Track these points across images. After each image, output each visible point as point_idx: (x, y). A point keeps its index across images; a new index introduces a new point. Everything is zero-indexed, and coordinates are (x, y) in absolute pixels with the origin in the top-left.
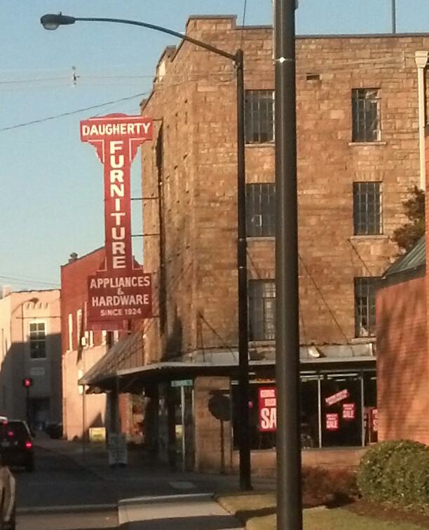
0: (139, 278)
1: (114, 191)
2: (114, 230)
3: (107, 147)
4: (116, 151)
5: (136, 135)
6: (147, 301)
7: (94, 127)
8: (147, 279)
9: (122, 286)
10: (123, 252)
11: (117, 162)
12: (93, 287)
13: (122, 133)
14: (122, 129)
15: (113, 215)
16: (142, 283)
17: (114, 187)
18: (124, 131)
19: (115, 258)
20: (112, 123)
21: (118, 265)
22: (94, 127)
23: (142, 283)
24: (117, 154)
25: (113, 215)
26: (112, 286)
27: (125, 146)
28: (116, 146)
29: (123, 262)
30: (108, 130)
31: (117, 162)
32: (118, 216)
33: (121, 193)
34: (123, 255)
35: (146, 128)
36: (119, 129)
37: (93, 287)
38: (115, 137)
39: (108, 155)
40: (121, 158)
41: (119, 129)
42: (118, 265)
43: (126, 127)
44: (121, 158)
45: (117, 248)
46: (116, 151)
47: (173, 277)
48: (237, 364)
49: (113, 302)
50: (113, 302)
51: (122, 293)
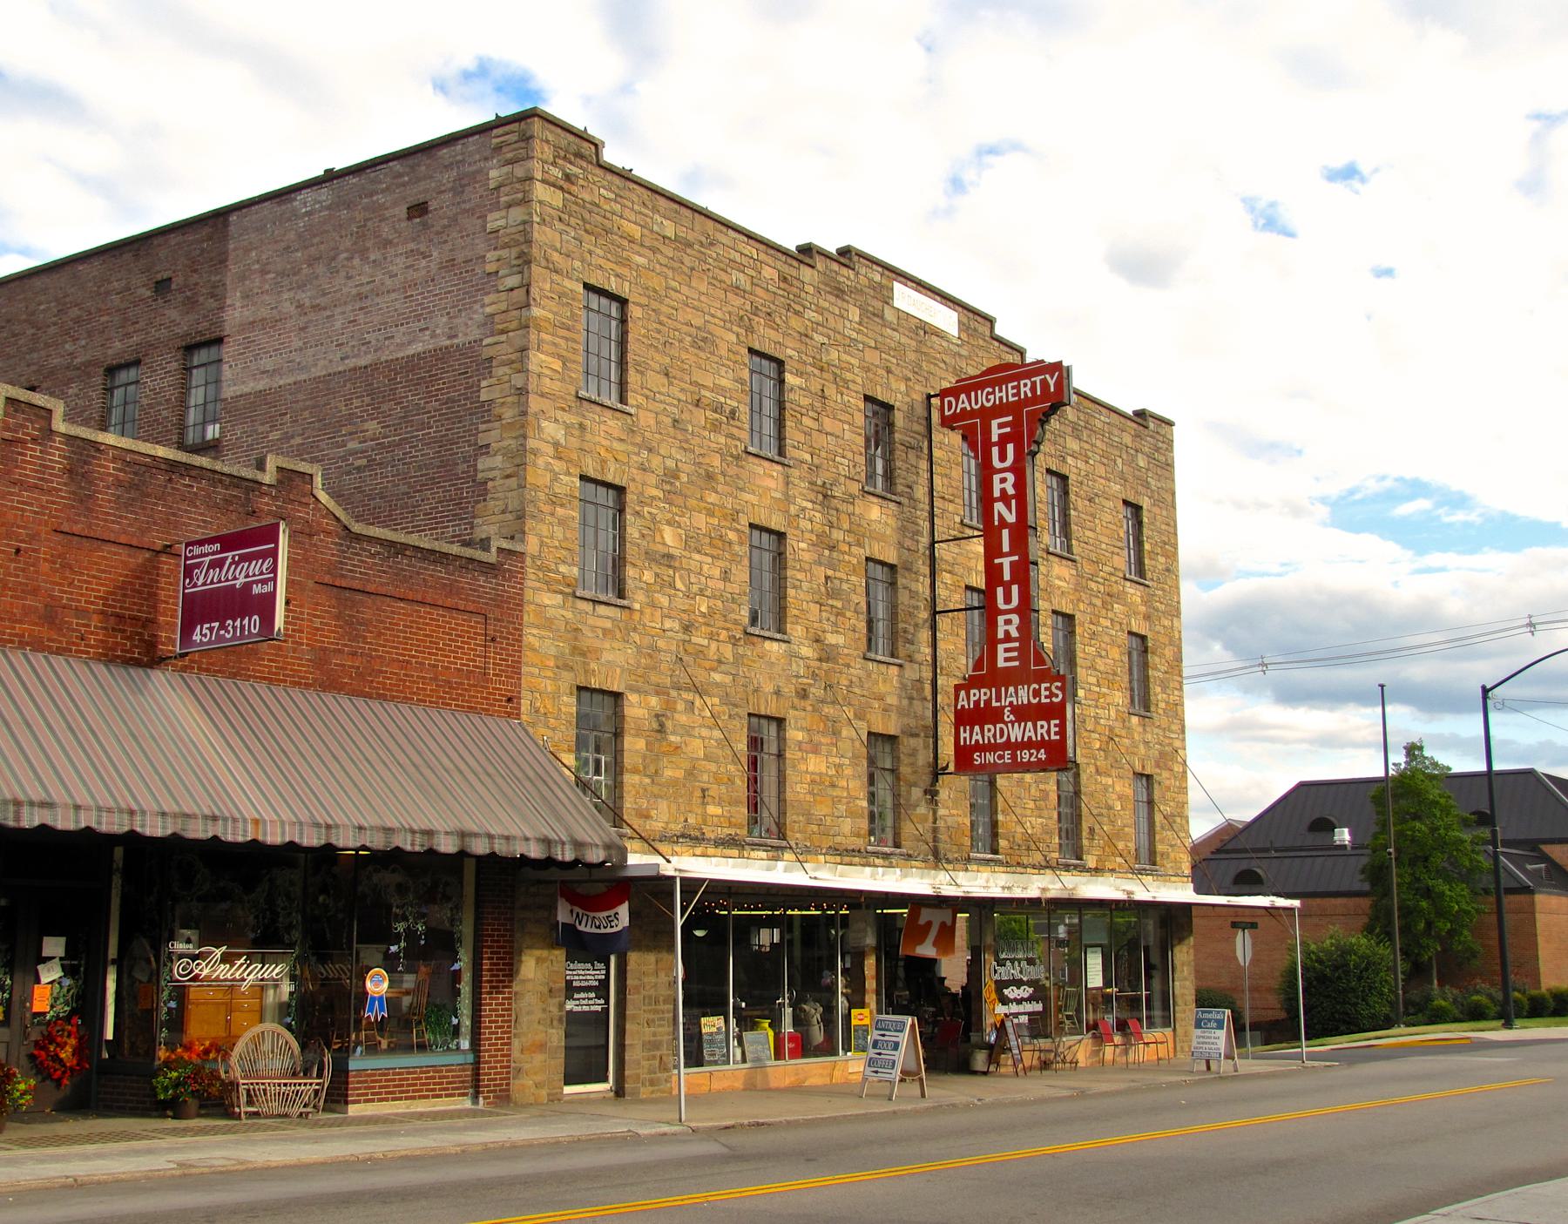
0: (1043, 686)
1: (999, 513)
2: (1000, 591)
3: (987, 431)
4: (1000, 435)
5: (1034, 399)
6: (1056, 733)
7: (963, 396)
8: (1057, 688)
9: (1011, 703)
10: (1015, 634)
11: (1003, 458)
12: (963, 706)
13: (1011, 399)
14: (1011, 392)
15: (997, 561)
16: (1046, 697)
17: (999, 507)
18: (1014, 395)
19: (1001, 647)
20: (992, 383)
21: (1007, 660)
22: (963, 396)
23: (1046, 697)
24: (1004, 440)
25: (997, 561)
26: (994, 704)
27: (1015, 425)
28: (1001, 426)
29: (1015, 654)
30: (984, 399)
31: (1003, 458)
32: (1006, 562)
33: (1011, 518)
34: (1015, 640)
35: (1052, 383)
36: (1006, 394)
37: (963, 706)
38: (999, 410)
39: (987, 445)
40: (1010, 448)
41: (1006, 394)
42: (1007, 660)
43: (1018, 387)
44: (1010, 448)
45: (1007, 627)
46: (1000, 435)
47: (582, 427)
48: (46, 939)
49: (995, 736)
50: (995, 736)
51: (1012, 718)
